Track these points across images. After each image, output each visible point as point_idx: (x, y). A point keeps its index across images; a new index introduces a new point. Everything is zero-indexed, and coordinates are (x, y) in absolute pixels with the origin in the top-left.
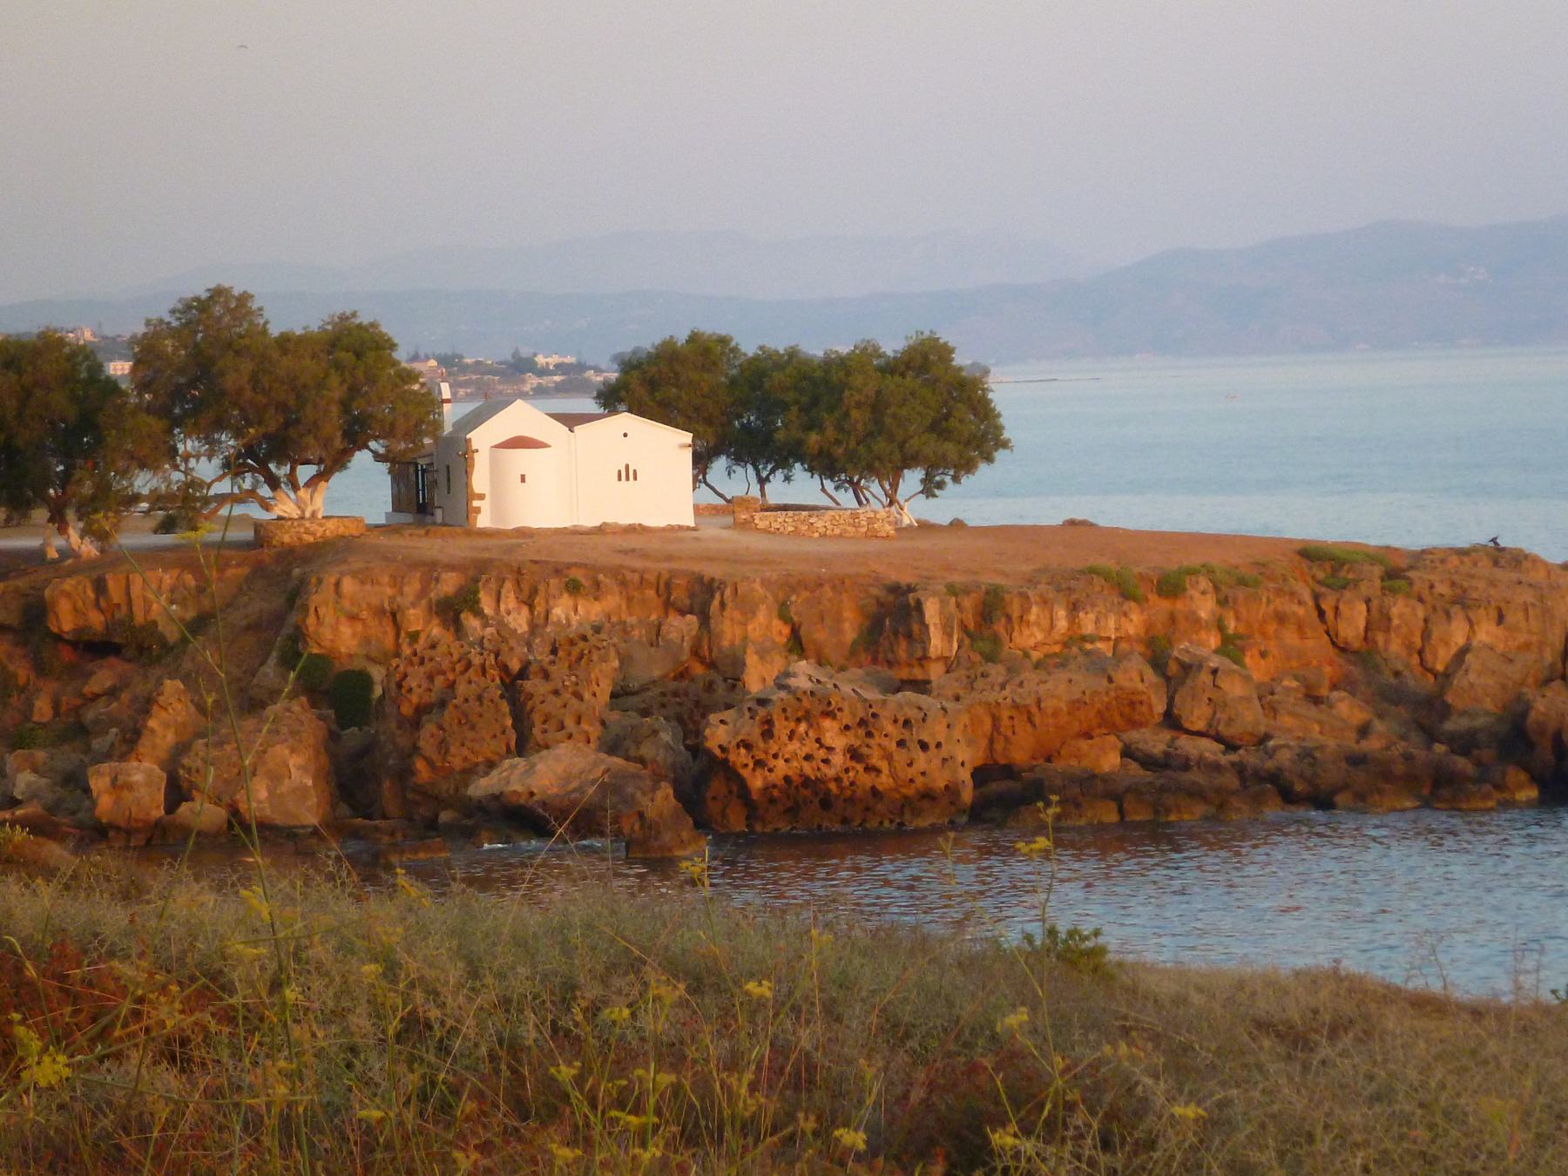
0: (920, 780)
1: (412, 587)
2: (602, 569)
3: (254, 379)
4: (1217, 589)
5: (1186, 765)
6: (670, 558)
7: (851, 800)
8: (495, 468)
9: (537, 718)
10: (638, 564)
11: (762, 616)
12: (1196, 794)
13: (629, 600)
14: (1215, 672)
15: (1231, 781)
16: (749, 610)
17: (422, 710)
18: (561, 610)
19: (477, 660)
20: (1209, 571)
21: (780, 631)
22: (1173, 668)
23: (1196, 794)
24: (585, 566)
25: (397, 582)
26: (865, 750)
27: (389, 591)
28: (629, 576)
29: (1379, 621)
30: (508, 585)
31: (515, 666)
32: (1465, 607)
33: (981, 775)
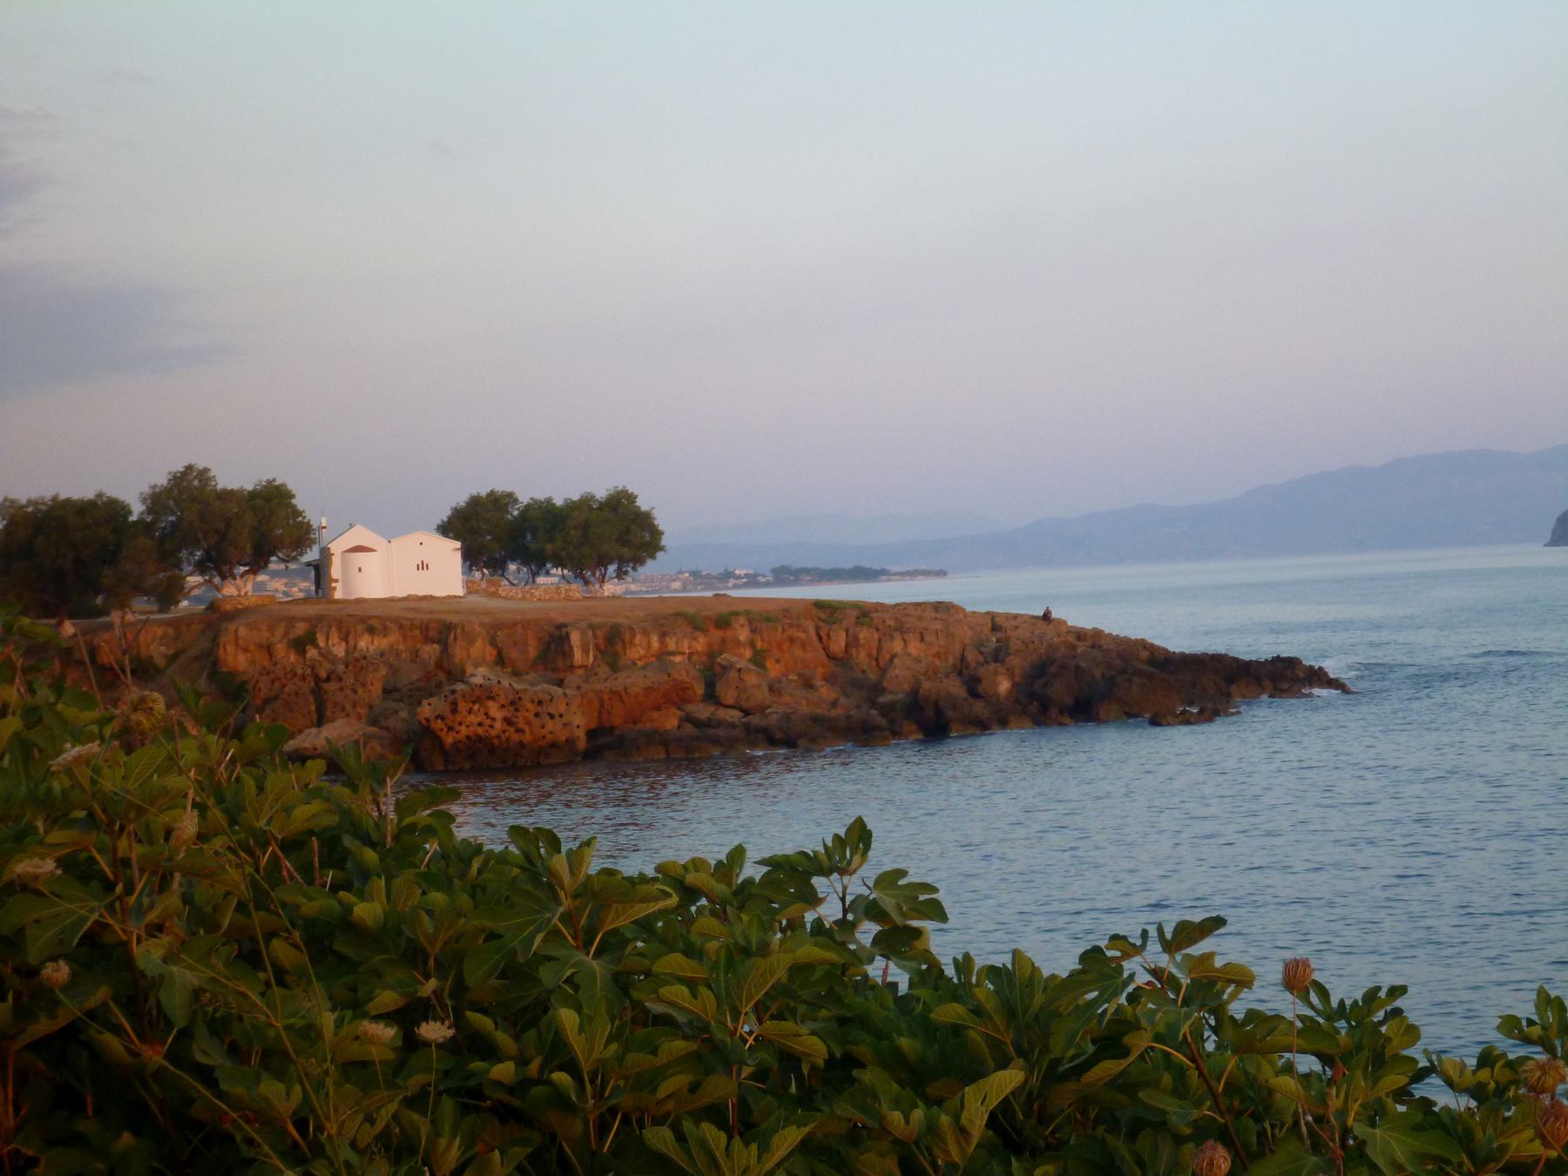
0: (549, 737)
1: (280, 631)
4: (750, 622)
5: (720, 724)
6: (432, 612)
9: (329, 705)
10: (410, 615)
11: (479, 644)
13: (405, 637)
14: (740, 670)
16: (472, 642)
17: (267, 701)
19: (300, 672)
20: (747, 613)
21: (491, 653)
22: (717, 669)
23: (716, 741)
25: (271, 629)
29: (852, 643)
31: (323, 675)
32: (902, 633)
33: (591, 734)
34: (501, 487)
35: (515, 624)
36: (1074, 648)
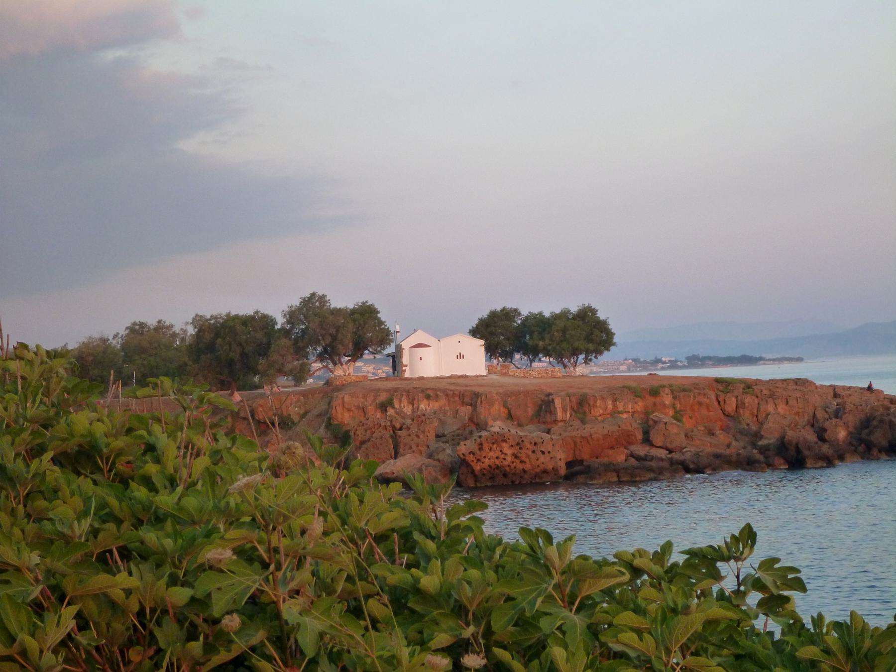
0: (542, 466)
1: (370, 399)
2: (440, 390)
3: (321, 325)
4: (672, 392)
5: (652, 458)
6: (466, 386)
7: (514, 474)
8: (411, 355)
9: (402, 445)
10: (453, 388)
11: (496, 406)
12: (651, 470)
13: (449, 401)
14: (666, 423)
15: (666, 464)
17: (363, 443)
18: (423, 406)
19: (383, 424)
20: (671, 386)
22: (651, 423)
23: (651, 470)
24: (433, 389)
25: (365, 397)
26: (519, 455)
27: (362, 400)
28: (449, 392)
29: (740, 405)
30: (404, 397)
31: (398, 426)
32: (774, 399)
33: (569, 465)
34: (510, 305)
35: (519, 393)
36: (888, 409)
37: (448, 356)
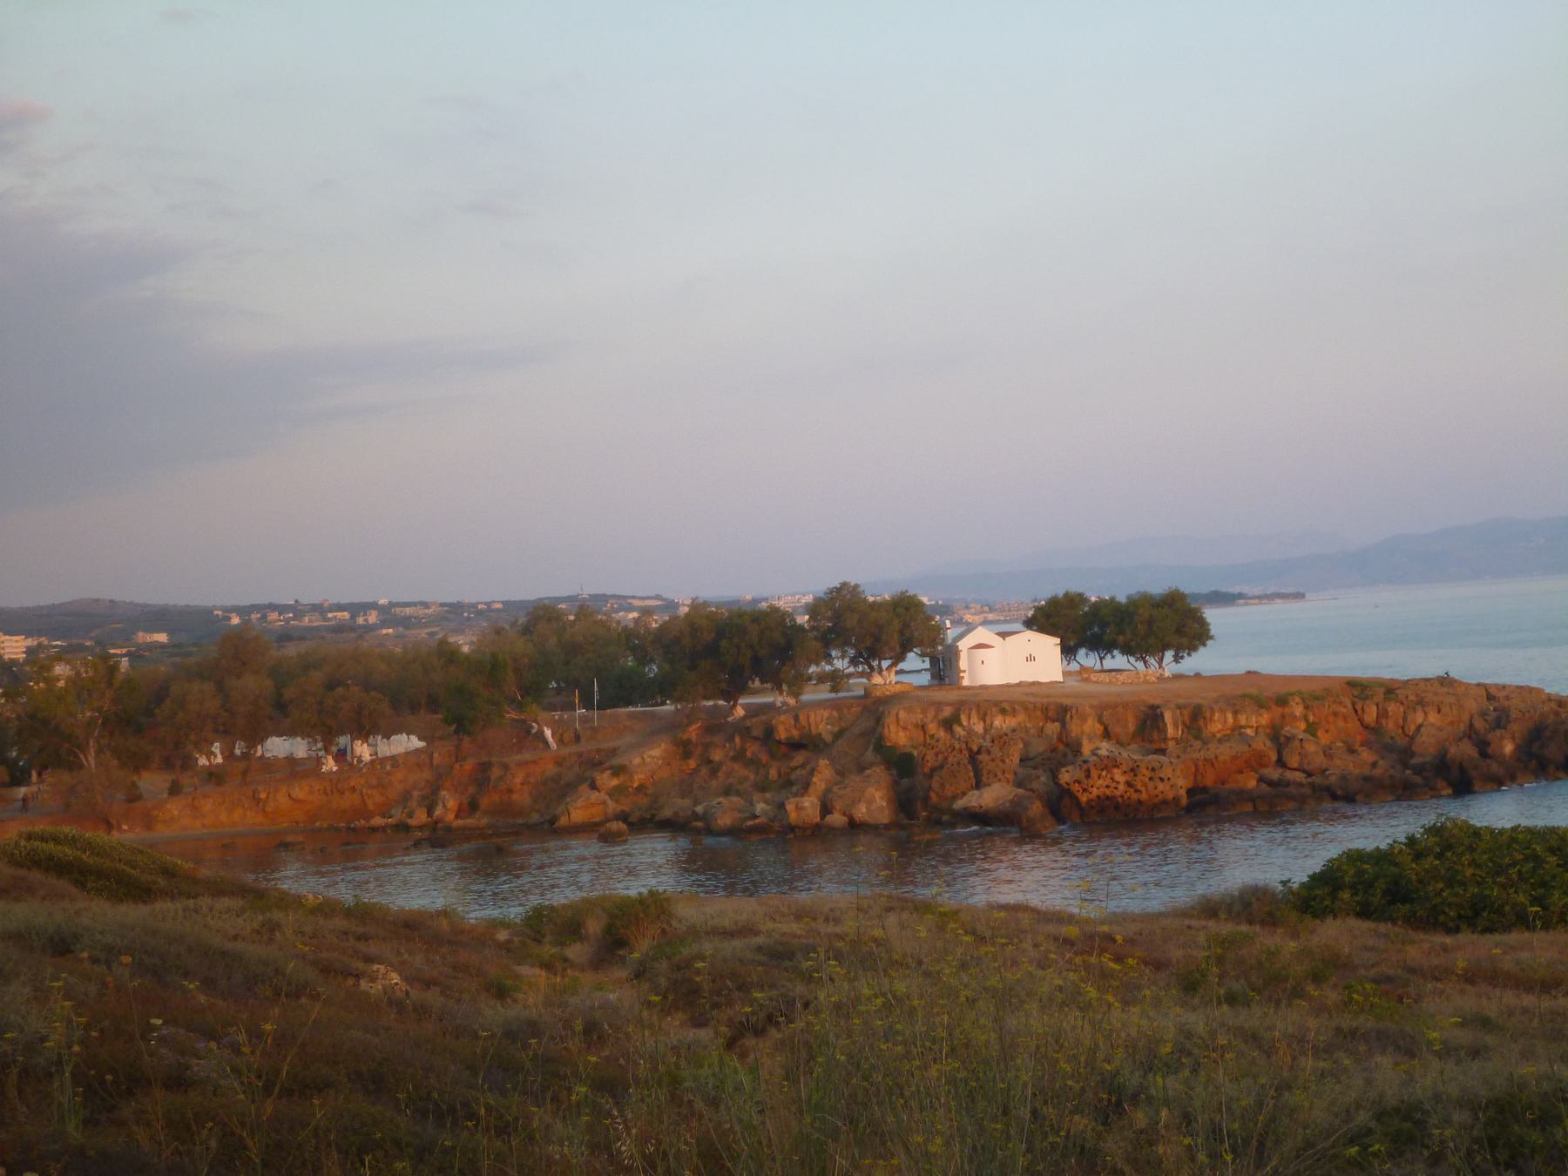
1: (930, 715)
5: (1288, 784)
10: (1032, 699)
11: (1090, 721)
15: (1307, 791)
16: (1084, 719)
17: (933, 770)
20: (1300, 693)
21: (1099, 728)
22: (1282, 739)
23: (1291, 798)
29: (1383, 714)
31: (975, 748)
33: (1189, 792)
34: (1075, 587)
35: (1117, 706)
36: (1557, 714)
37: (1010, 661)
